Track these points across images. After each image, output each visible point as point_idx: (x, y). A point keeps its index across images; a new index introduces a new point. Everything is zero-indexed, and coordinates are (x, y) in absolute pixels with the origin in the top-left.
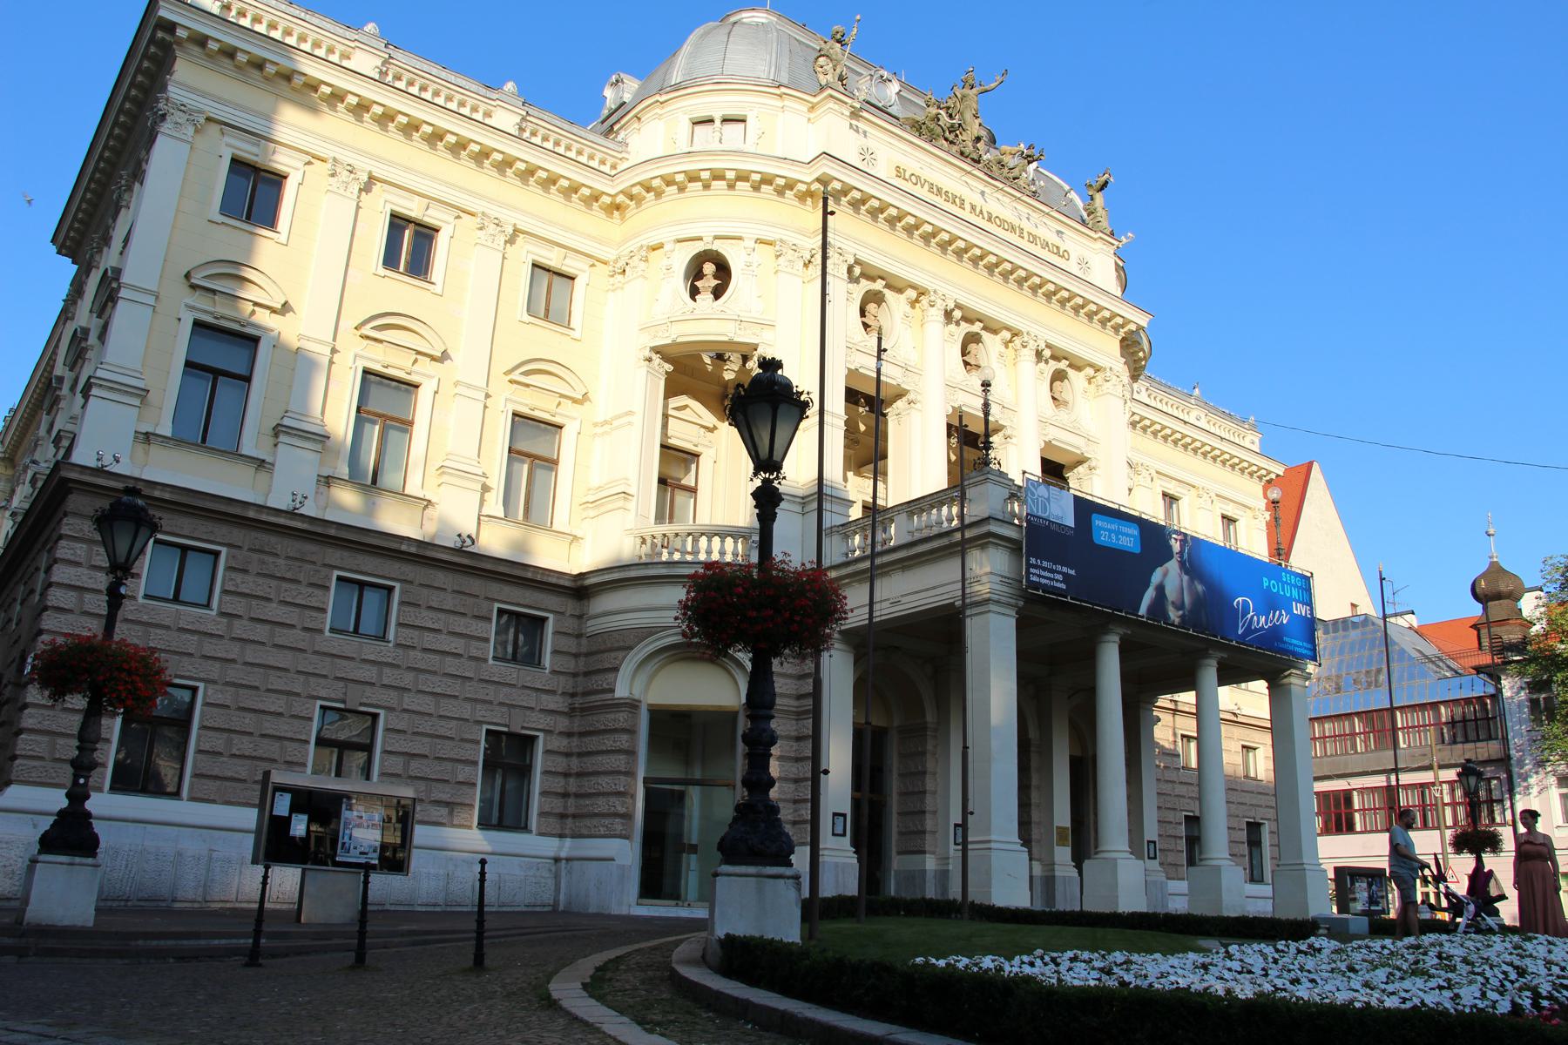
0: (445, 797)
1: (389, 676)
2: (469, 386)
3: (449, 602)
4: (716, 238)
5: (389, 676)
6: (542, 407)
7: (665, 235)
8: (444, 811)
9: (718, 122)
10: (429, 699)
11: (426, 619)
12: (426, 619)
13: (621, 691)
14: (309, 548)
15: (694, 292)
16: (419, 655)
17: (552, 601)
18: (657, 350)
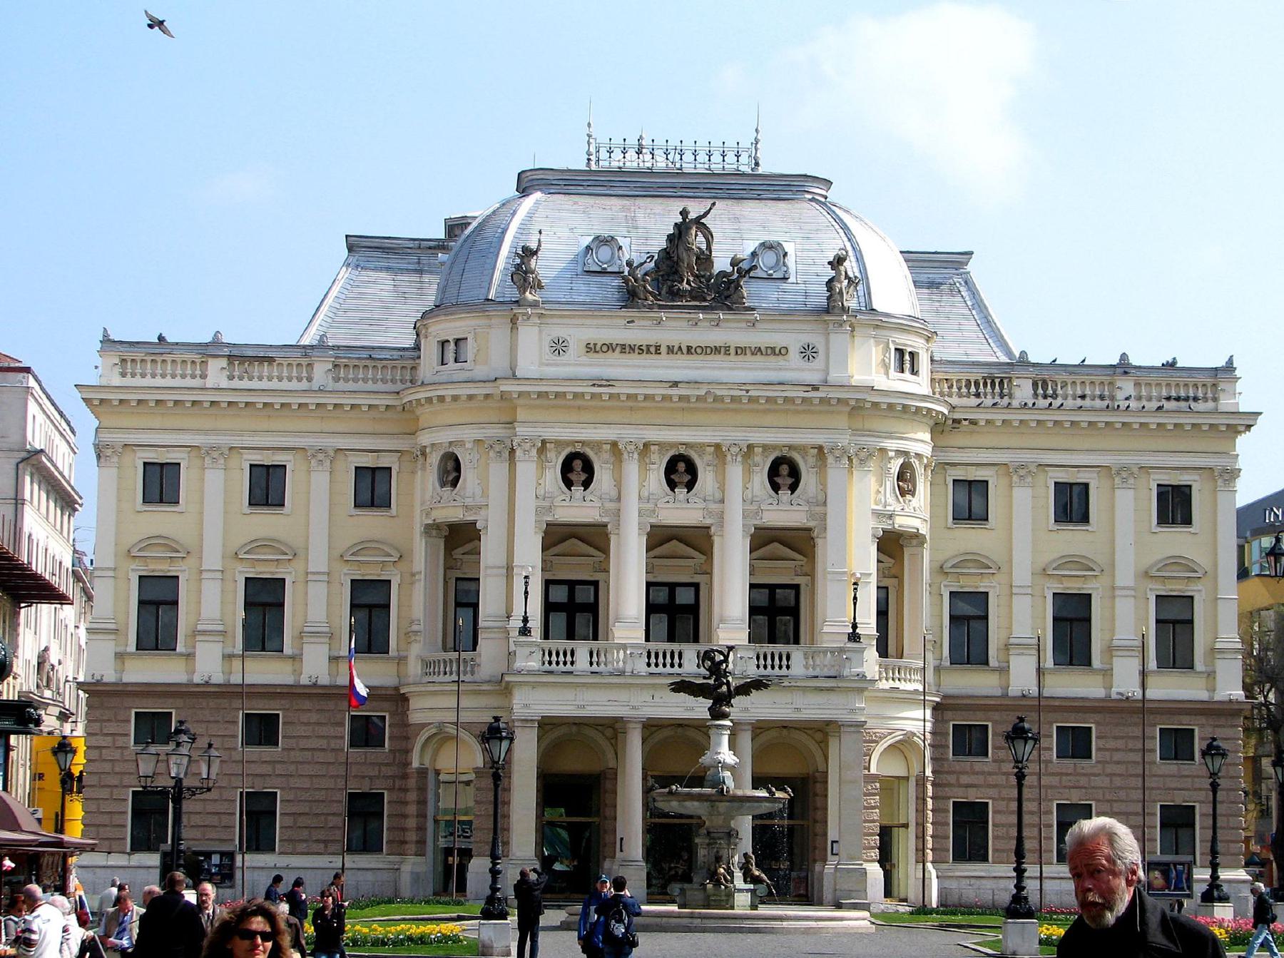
0: (322, 838)
1: (280, 769)
2: (314, 573)
3: (314, 717)
4: (451, 443)
5: (280, 769)
6: (372, 574)
7: (425, 439)
8: (322, 846)
9: (452, 346)
10: (306, 780)
11: (301, 731)
12: (301, 731)
13: (415, 764)
14: (224, 702)
15: (443, 485)
16: (298, 753)
17: (386, 705)
18: (428, 527)
